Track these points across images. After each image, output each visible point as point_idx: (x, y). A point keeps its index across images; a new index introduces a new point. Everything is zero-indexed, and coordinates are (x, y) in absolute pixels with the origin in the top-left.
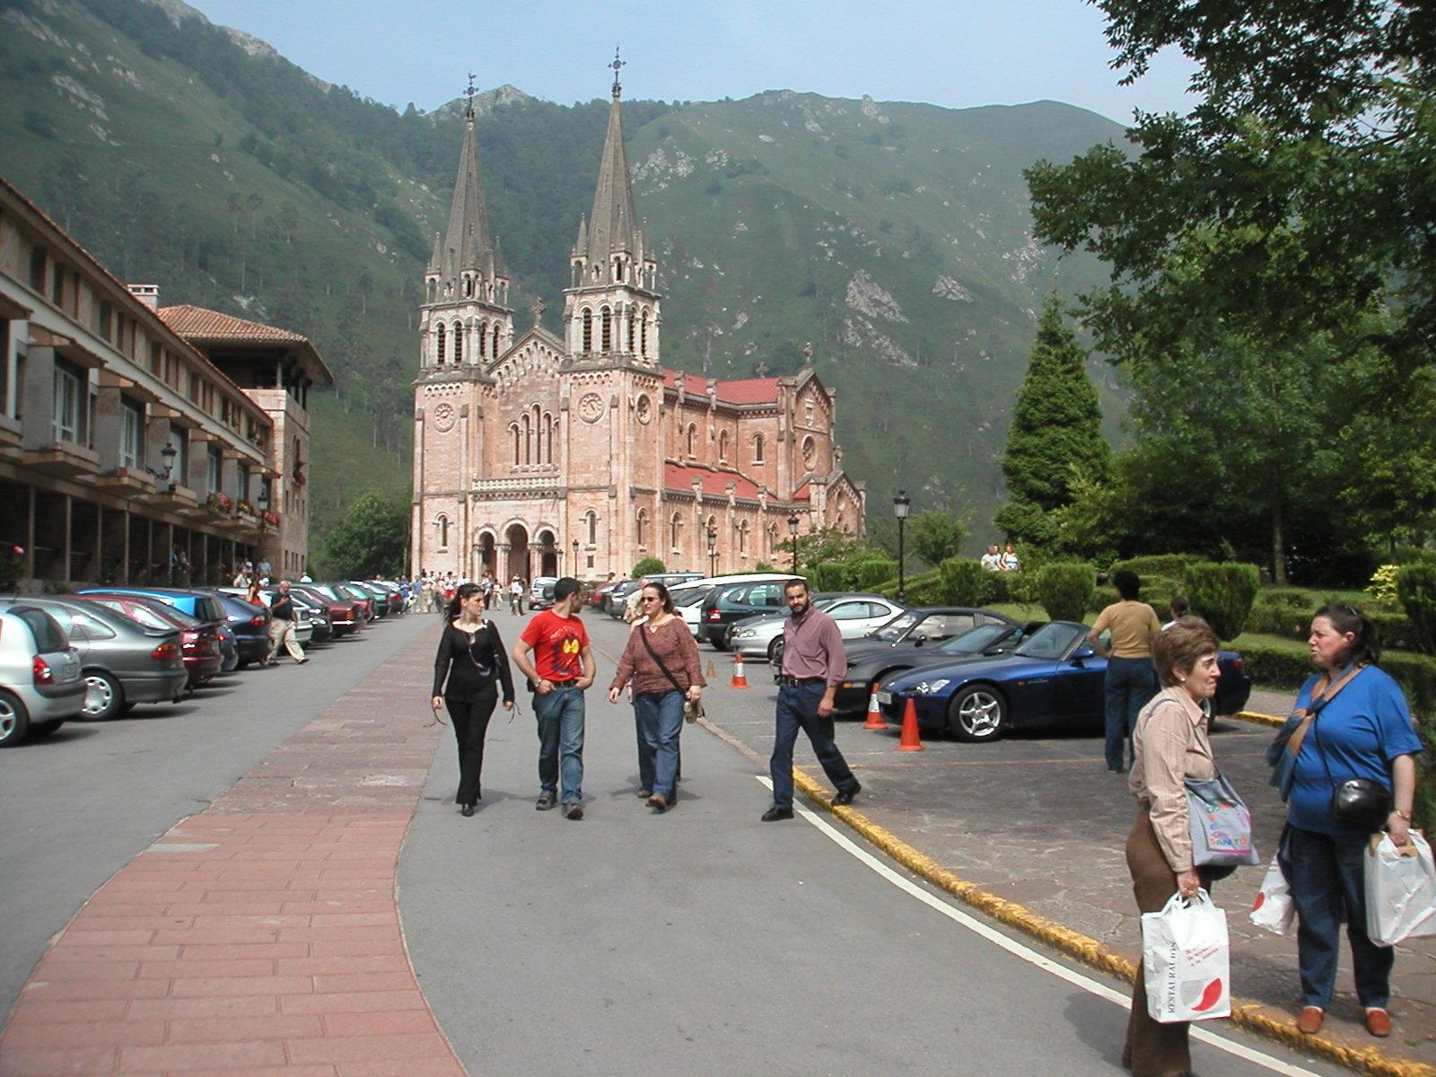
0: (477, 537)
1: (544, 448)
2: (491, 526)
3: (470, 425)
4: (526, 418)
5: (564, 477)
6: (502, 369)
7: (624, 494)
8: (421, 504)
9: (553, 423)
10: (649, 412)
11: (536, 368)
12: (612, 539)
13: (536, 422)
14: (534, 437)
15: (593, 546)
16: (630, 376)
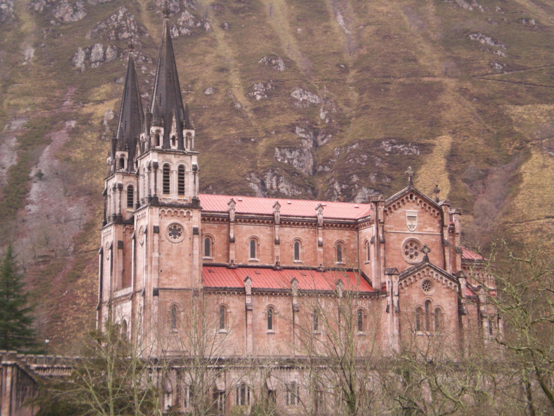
3: (114, 254)
7: (149, 293)
10: (182, 234)
16: (156, 211)
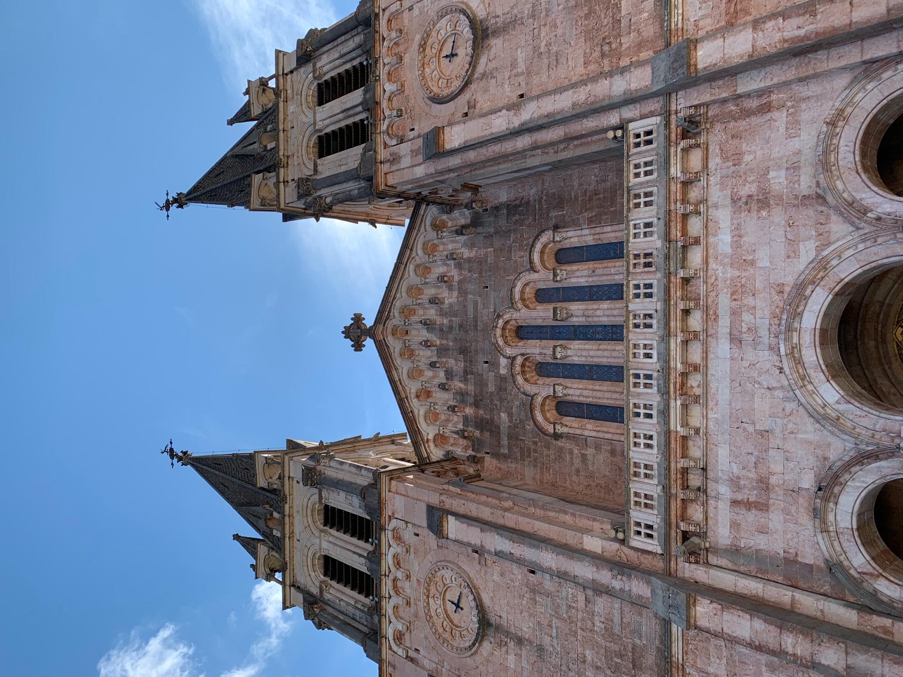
2: (828, 487)
3: (473, 509)
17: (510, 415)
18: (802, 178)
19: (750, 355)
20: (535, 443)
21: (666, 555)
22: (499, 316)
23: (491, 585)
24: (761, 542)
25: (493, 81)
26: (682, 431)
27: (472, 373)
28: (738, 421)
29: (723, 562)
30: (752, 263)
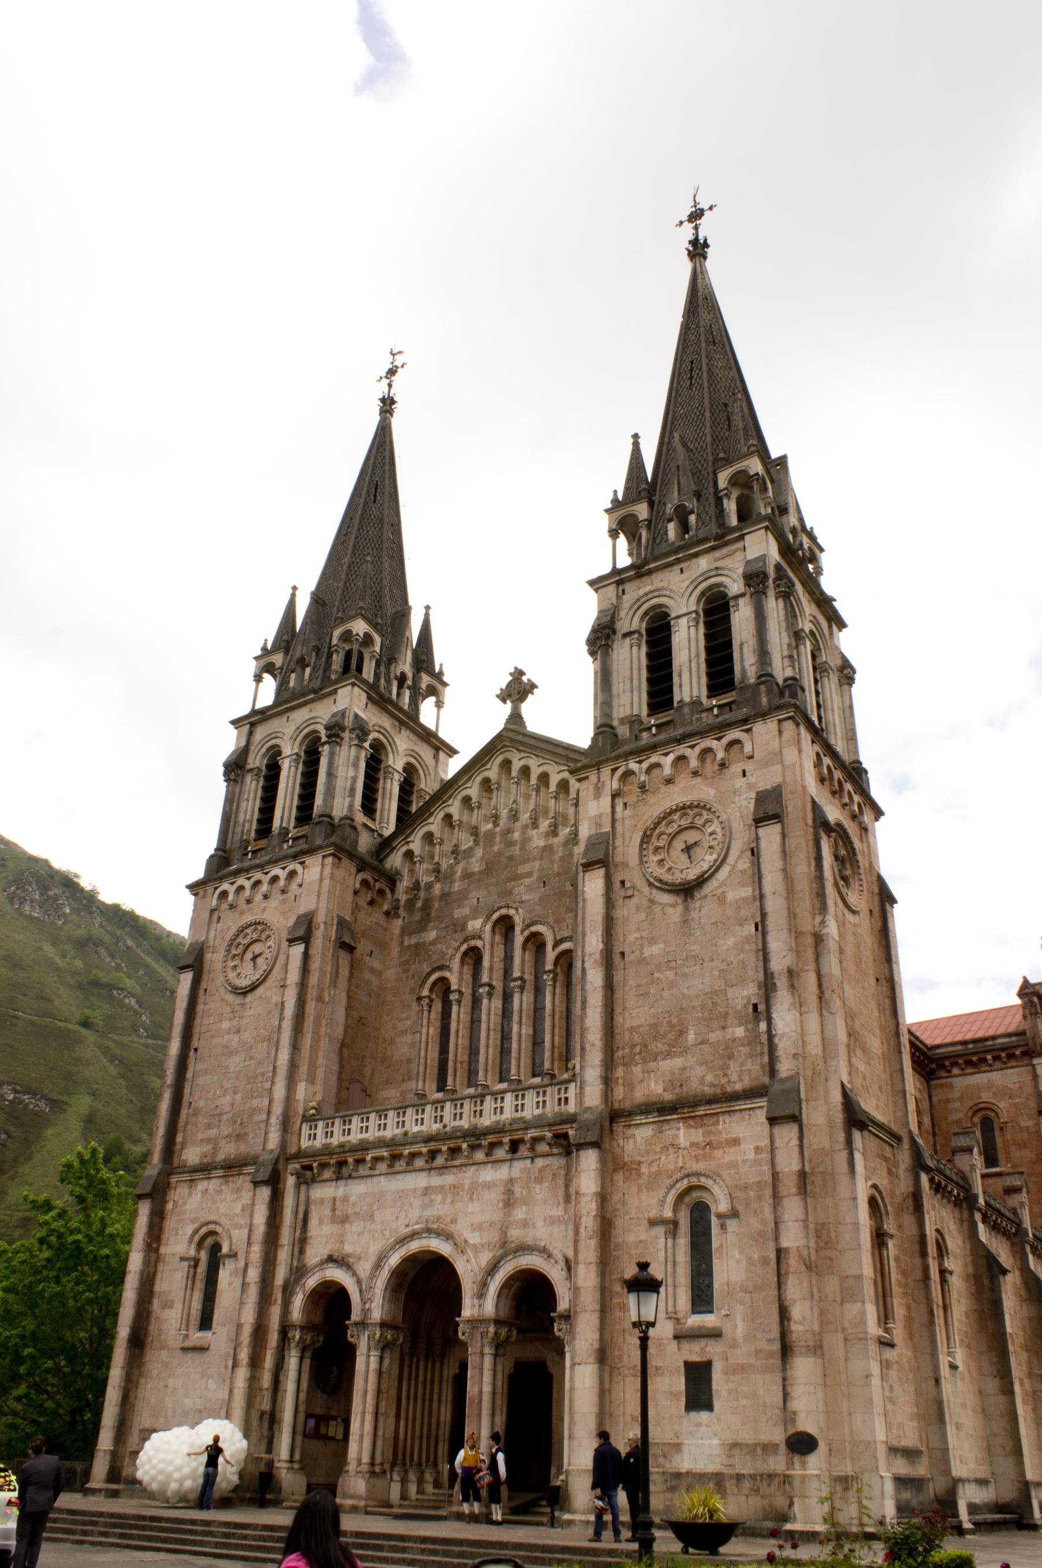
0: (298, 1301)
1: (521, 1030)
3: (315, 964)
4: (473, 956)
5: (592, 1074)
6: (416, 844)
8: (158, 1194)
9: (551, 955)
11: (503, 821)
12: (795, 1289)
13: (499, 966)
14: (491, 1008)
15: (709, 1320)
17: (435, 942)
18: (518, 1231)
19: (417, 1203)
20: (413, 977)
21: (299, 1155)
22: (517, 909)
23: (269, 994)
24: (313, 1222)
25: (643, 917)
26: (368, 1158)
27: (469, 885)
28: (380, 1197)
29: (302, 1196)
30: (471, 1199)
